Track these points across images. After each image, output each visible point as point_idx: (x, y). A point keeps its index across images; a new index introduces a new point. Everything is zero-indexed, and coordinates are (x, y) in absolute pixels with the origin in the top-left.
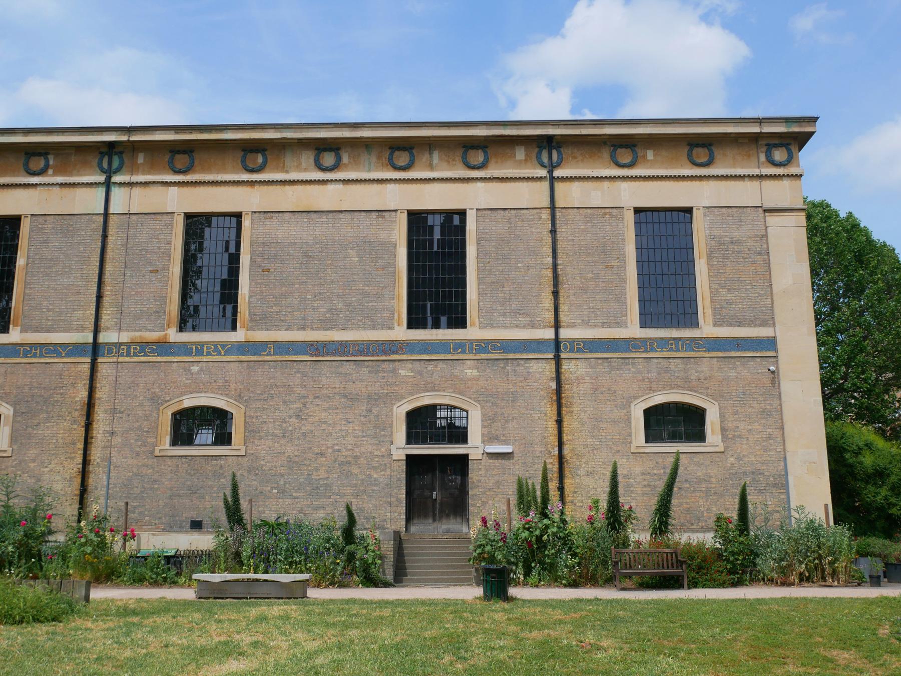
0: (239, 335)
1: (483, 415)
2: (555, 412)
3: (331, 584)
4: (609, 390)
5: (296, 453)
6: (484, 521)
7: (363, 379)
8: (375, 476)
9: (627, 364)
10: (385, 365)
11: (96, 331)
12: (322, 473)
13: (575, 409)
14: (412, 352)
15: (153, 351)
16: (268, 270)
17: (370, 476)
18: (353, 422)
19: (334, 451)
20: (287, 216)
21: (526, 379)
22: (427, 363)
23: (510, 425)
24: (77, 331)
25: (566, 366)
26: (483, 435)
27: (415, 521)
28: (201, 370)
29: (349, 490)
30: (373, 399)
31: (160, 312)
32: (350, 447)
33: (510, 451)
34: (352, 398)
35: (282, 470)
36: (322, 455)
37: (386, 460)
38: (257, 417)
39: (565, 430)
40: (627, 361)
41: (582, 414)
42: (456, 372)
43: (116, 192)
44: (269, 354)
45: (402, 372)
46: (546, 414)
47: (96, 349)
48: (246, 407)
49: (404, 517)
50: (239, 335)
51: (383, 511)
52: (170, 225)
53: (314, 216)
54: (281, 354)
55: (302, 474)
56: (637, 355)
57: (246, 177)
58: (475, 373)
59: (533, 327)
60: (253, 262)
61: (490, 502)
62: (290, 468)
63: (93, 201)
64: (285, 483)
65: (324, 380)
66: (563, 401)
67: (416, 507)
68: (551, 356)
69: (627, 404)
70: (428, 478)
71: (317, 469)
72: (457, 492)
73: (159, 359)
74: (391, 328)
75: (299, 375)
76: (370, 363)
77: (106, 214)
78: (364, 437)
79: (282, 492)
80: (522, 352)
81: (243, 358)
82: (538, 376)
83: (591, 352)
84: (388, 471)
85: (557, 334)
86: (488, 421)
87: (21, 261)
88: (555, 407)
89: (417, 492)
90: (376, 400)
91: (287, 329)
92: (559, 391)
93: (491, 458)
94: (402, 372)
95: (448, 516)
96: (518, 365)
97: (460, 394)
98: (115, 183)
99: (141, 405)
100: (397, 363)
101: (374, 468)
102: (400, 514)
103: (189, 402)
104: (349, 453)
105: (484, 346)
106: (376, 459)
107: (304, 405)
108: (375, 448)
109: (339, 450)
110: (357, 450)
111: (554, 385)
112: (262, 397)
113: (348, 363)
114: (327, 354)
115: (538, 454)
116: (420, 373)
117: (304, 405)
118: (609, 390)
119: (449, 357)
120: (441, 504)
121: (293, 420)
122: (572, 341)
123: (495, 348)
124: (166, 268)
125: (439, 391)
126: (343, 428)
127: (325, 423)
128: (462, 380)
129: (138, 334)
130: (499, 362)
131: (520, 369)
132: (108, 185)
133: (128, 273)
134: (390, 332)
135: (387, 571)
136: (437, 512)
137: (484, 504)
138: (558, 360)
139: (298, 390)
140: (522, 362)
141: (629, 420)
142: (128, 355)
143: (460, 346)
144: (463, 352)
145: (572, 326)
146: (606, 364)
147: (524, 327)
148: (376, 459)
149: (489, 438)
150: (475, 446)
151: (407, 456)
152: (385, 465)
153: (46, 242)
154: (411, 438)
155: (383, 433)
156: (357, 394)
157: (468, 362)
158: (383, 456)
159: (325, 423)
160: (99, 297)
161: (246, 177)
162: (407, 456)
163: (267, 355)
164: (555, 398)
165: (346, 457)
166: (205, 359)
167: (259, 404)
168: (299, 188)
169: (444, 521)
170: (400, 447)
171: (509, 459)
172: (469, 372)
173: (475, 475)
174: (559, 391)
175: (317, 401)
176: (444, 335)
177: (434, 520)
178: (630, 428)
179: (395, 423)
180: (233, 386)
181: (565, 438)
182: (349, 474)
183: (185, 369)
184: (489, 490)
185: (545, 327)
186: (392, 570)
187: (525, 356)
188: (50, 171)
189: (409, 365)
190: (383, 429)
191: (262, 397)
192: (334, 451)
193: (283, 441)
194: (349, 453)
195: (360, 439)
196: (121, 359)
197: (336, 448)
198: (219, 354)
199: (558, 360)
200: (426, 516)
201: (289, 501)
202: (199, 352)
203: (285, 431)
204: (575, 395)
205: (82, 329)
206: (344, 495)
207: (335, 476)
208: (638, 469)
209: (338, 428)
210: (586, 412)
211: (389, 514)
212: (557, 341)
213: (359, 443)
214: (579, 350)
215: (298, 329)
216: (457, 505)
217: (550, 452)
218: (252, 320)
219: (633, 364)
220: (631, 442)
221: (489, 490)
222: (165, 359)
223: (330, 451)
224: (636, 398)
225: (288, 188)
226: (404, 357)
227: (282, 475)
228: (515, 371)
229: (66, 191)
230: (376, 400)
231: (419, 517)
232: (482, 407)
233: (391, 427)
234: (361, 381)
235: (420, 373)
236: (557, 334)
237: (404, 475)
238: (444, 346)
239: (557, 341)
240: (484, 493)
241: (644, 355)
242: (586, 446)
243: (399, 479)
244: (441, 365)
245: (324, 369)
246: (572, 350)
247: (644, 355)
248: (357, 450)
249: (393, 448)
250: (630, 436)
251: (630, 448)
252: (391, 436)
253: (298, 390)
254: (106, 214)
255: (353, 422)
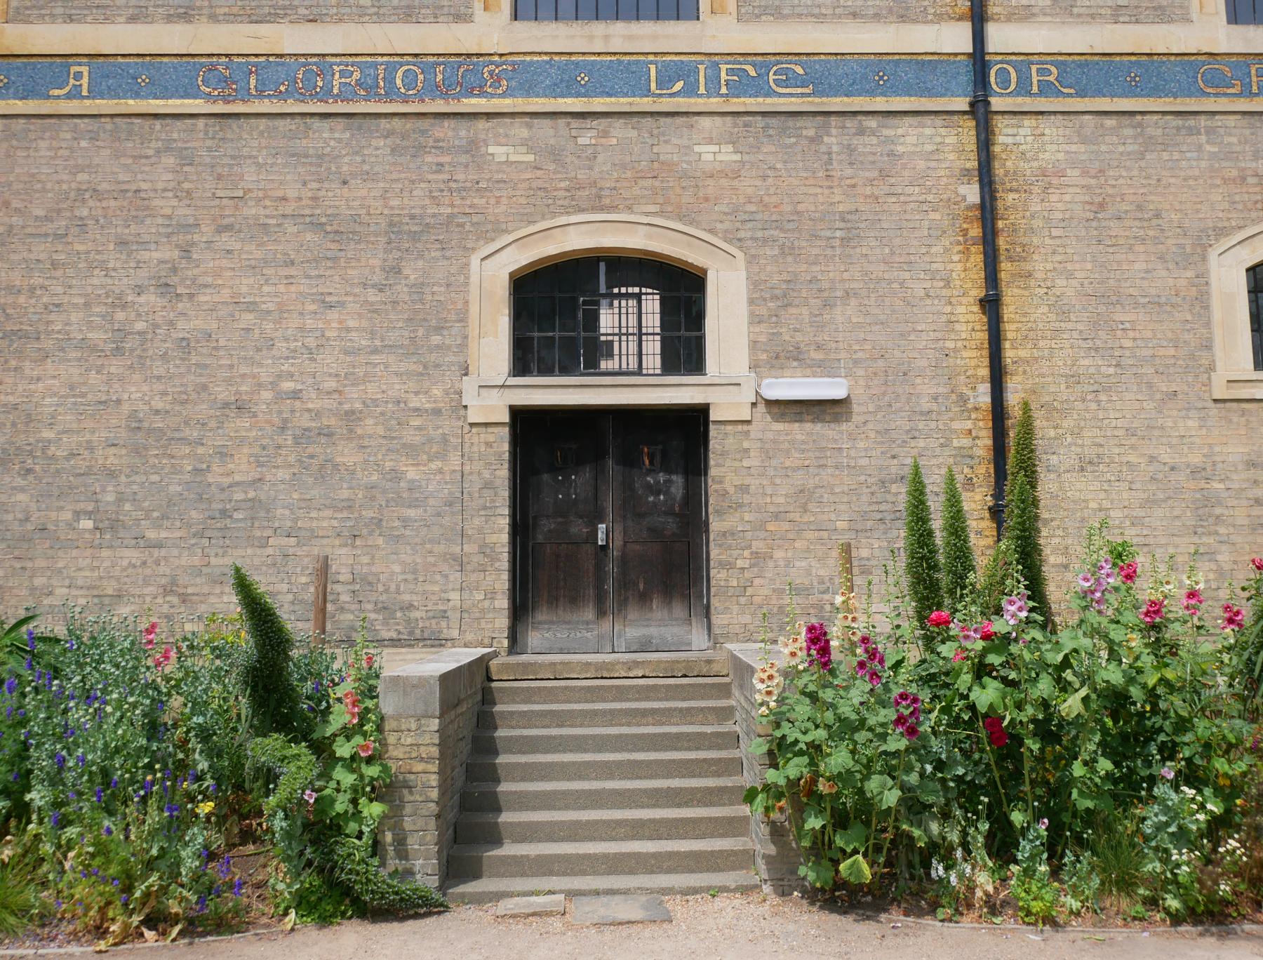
1: (755, 284)
2: (978, 274)
3: (150, 922)
4: (1140, 208)
5: (158, 404)
6: (818, 638)
7: (376, 178)
8: (412, 474)
9: (1192, 131)
10: (445, 130)
12: (242, 468)
13: (1039, 265)
14: (528, 90)
17: (396, 476)
18: (342, 304)
19: (280, 397)
21: (884, 175)
22: (575, 123)
23: (838, 314)
25: (1006, 135)
26: (754, 345)
27: (542, 615)
29: (325, 521)
30: (405, 234)
32: (331, 384)
33: (840, 393)
34: (340, 233)
35: (113, 458)
36: (240, 408)
37: (448, 425)
38: (32, 290)
39: (1010, 330)
40: (1191, 122)
41: (1060, 282)
42: (667, 152)
44: (75, 94)
45: (498, 152)
46: (948, 283)
49: (503, 603)
51: (420, 595)
54: (113, 93)
55: (176, 470)
56: (1223, 104)
58: (727, 155)
59: (903, 18)
61: (779, 554)
62: (137, 451)
64: (120, 500)
65: (250, 175)
66: (1002, 242)
67: (542, 574)
68: (962, 104)
69: (1195, 254)
70: (581, 481)
71: (223, 455)
72: (671, 525)
74: (462, 17)
75: (169, 161)
76: (397, 123)
78: (375, 351)
79: (110, 526)
80: (871, 93)
82: (922, 164)
83: (1081, 94)
84: (454, 461)
85: (979, 38)
86: (769, 301)
88: (977, 258)
89: (547, 526)
90: (414, 237)
91: (132, 19)
92: (988, 212)
93: (778, 418)
94: (498, 152)
95: (644, 599)
96: (861, 132)
97: (680, 218)
100: (481, 124)
101: (410, 450)
102: (491, 595)
104: (328, 403)
105: (753, 72)
106: (416, 422)
107: (186, 251)
108: (412, 385)
109: (296, 395)
110: (353, 393)
111: (972, 193)
112: (49, 228)
113: (326, 124)
114: (260, 95)
115: (925, 405)
116: (555, 154)
117: (186, 251)
118: (1140, 208)
119: (645, 104)
120: (624, 561)
121: (150, 298)
122: (1024, 60)
123: (789, 80)
125: (612, 208)
126: (310, 323)
127: (251, 307)
128: (685, 175)
130: (800, 122)
131: (866, 144)
134: (460, 29)
135: (413, 843)
136: (609, 586)
137: (759, 559)
138: (980, 112)
139: (165, 205)
140: (872, 123)
141: (1201, 301)
143: (678, 71)
144: (690, 90)
145: (1025, 15)
146: (1128, 132)
147: (877, 17)
148: (416, 422)
149: (774, 355)
150: (730, 379)
151: (518, 414)
152: (445, 440)
154: (525, 359)
155: (436, 339)
156: (355, 219)
157: (705, 122)
158: (437, 412)
159: (251, 307)
162: (518, 414)
163: (69, 96)
164: (976, 231)
165: (318, 414)
167: (40, 250)
169: (633, 614)
170: (492, 384)
171: (836, 419)
172: (707, 152)
173: (727, 467)
174: (988, 212)
175: (226, 240)
176: (630, 38)
177: (601, 613)
178: (1208, 325)
179: (474, 309)
181: (1009, 354)
182: (326, 470)
184: (776, 516)
185: (939, 18)
186: (432, 835)
187: (880, 103)
189: (519, 130)
190: (433, 329)
191: (49, 228)
192: (280, 397)
193: (115, 366)
194: (328, 403)
195: (362, 359)
197: (288, 385)
199: (980, 112)
200: (575, 600)
201: (133, 555)
203: (123, 332)
204: (1037, 223)
206: (314, 535)
207: (282, 474)
208: (1234, 451)
209: (294, 322)
210: (1070, 276)
211: (454, 596)
212: (979, 58)
213: (360, 372)
214: (1046, 89)
215: (169, 19)
216: (674, 567)
217: (963, 399)
219: (1210, 131)
220: (1211, 368)
221: (776, 516)
223: (267, 395)
224: (1222, 232)
226: (506, 104)
227: (112, 474)
228: (851, 149)
230: (414, 237)
231: (553, 601)
232: (751, 260)
233: (463, 319)
234: (368, 177)
235: (555, 154)
236: (979, 38)
237: (504, 473)
238: (624, 72)
239: (979, 58)
240: (762, 526)
241: (1243, 105)
242: (1074, 379)
243: (488, 485)
244: (619, 130)
245: (250, 138)
246: (1024, 89)
247: (1243, 105)
248: (353, 393)
249: (469, 386)
250: (1209, 347)
251: (1208, 383)
252: (463, 346)
253: (165, 205)
255: (342, 304)
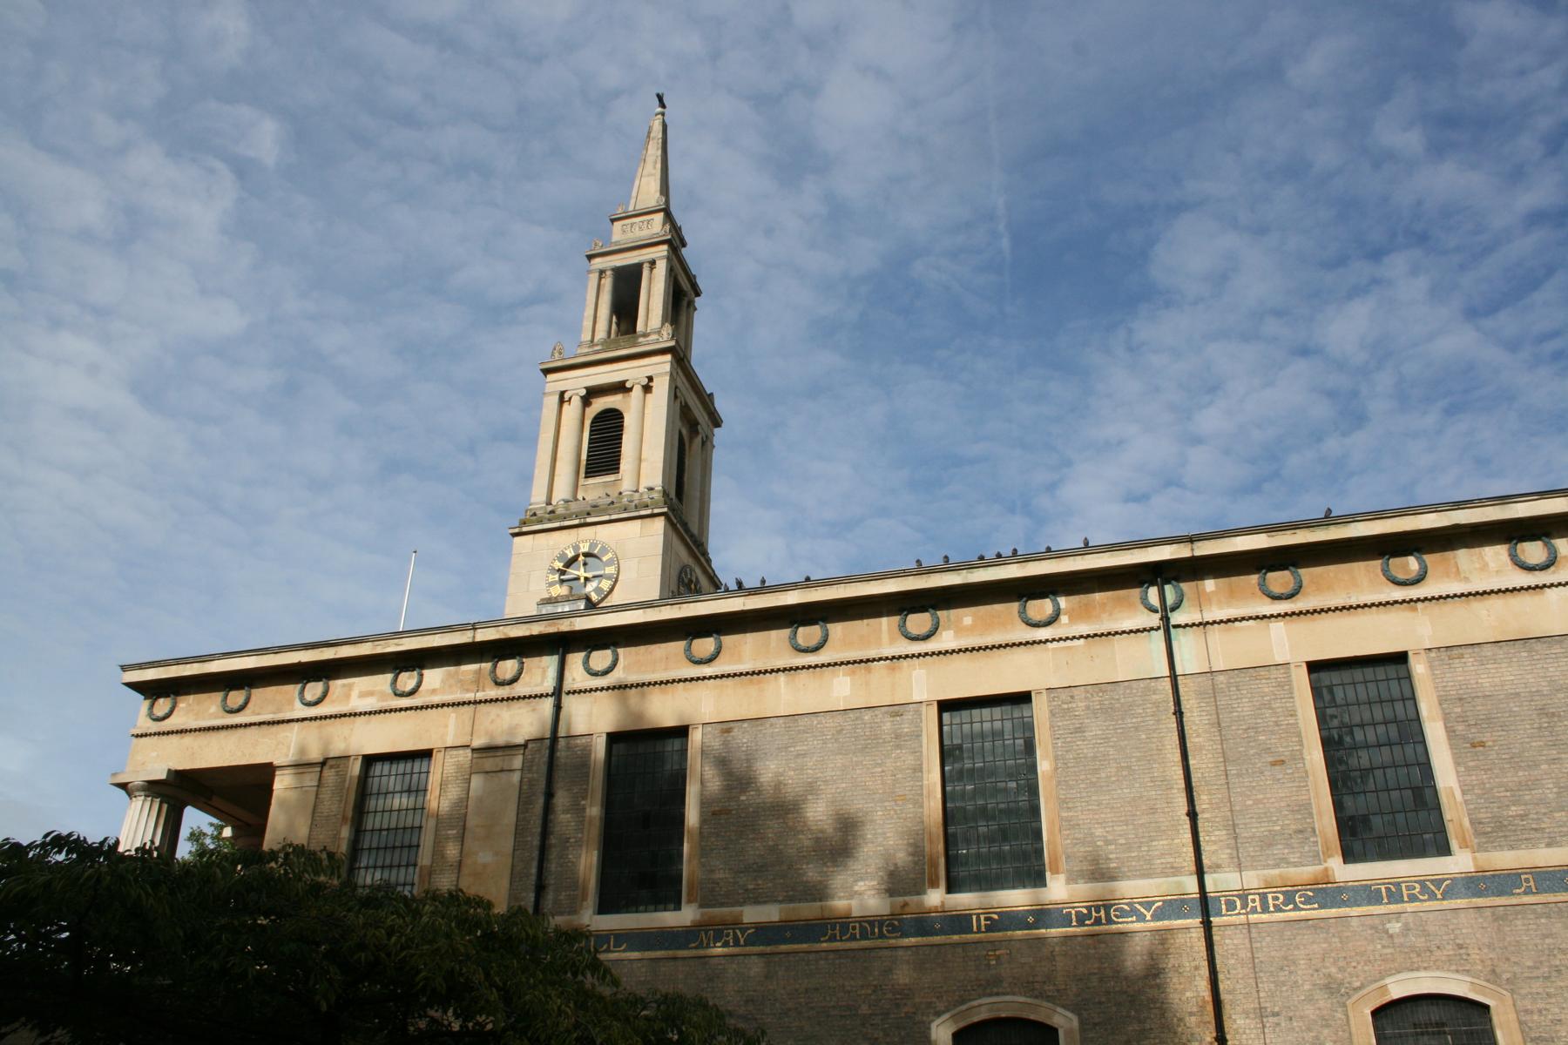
0: (1460, 862)
11: (1200, 873)
15: (1308, 901)
16: (1482, 744)
20: (1488, 651)
24: (1164, 874)
28: (1406, 929)
31: (1306, 832)
43: (1182, 641)
44: (1528, 892)
47: (1205, 905)
48: (1512, 992)
50: (1460, 862)
52: (1286, 685)
53: (1538, 646)
57: (1399, 594)
60: (1450, 732)
63: (1149, 657)
73: (1324, 913)
77: (1174, 677)
81: (1480, 901)
87: (1044, 766)
91: (1549, 845)
98: (1176, 627)
99: (1310, 999)
103: (1399, 988)
112: (1536, 973)
124: (1298, 757)
129: (1276, 872)
132: (1167, 627)
133: (1233, 770)
142: (1265, 909)
153: (1080, 730)
160: (1193, 815)
161: (1399, 594)
163: (1525, 893)
166: (1410, 907)
168: (1495, 602)
180: (1475, 955)
183: (1373, 927)
188: (1064, 619)
191: (1536, 973)
196: (1253, 917)
198: (1432, 897)
202: (1395, 896)
205: (1176, 871)
218: (1477, 834)
222: (1334, 912)
225: (1477, 605)
229: (1099, 646)
254: (1174, 677)
